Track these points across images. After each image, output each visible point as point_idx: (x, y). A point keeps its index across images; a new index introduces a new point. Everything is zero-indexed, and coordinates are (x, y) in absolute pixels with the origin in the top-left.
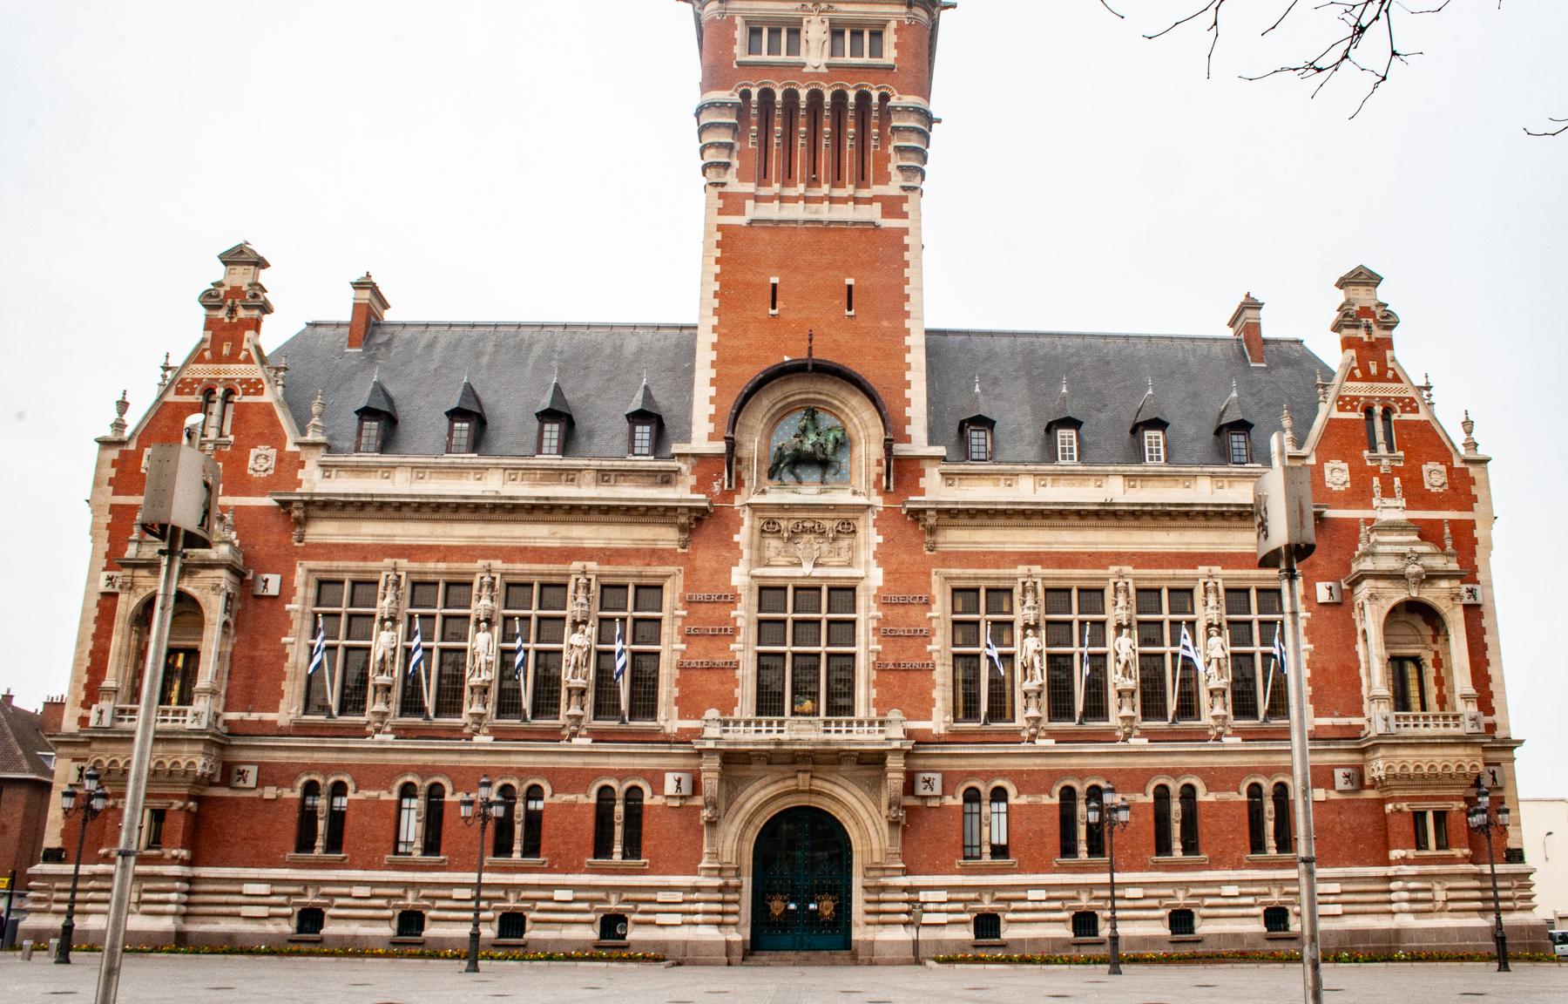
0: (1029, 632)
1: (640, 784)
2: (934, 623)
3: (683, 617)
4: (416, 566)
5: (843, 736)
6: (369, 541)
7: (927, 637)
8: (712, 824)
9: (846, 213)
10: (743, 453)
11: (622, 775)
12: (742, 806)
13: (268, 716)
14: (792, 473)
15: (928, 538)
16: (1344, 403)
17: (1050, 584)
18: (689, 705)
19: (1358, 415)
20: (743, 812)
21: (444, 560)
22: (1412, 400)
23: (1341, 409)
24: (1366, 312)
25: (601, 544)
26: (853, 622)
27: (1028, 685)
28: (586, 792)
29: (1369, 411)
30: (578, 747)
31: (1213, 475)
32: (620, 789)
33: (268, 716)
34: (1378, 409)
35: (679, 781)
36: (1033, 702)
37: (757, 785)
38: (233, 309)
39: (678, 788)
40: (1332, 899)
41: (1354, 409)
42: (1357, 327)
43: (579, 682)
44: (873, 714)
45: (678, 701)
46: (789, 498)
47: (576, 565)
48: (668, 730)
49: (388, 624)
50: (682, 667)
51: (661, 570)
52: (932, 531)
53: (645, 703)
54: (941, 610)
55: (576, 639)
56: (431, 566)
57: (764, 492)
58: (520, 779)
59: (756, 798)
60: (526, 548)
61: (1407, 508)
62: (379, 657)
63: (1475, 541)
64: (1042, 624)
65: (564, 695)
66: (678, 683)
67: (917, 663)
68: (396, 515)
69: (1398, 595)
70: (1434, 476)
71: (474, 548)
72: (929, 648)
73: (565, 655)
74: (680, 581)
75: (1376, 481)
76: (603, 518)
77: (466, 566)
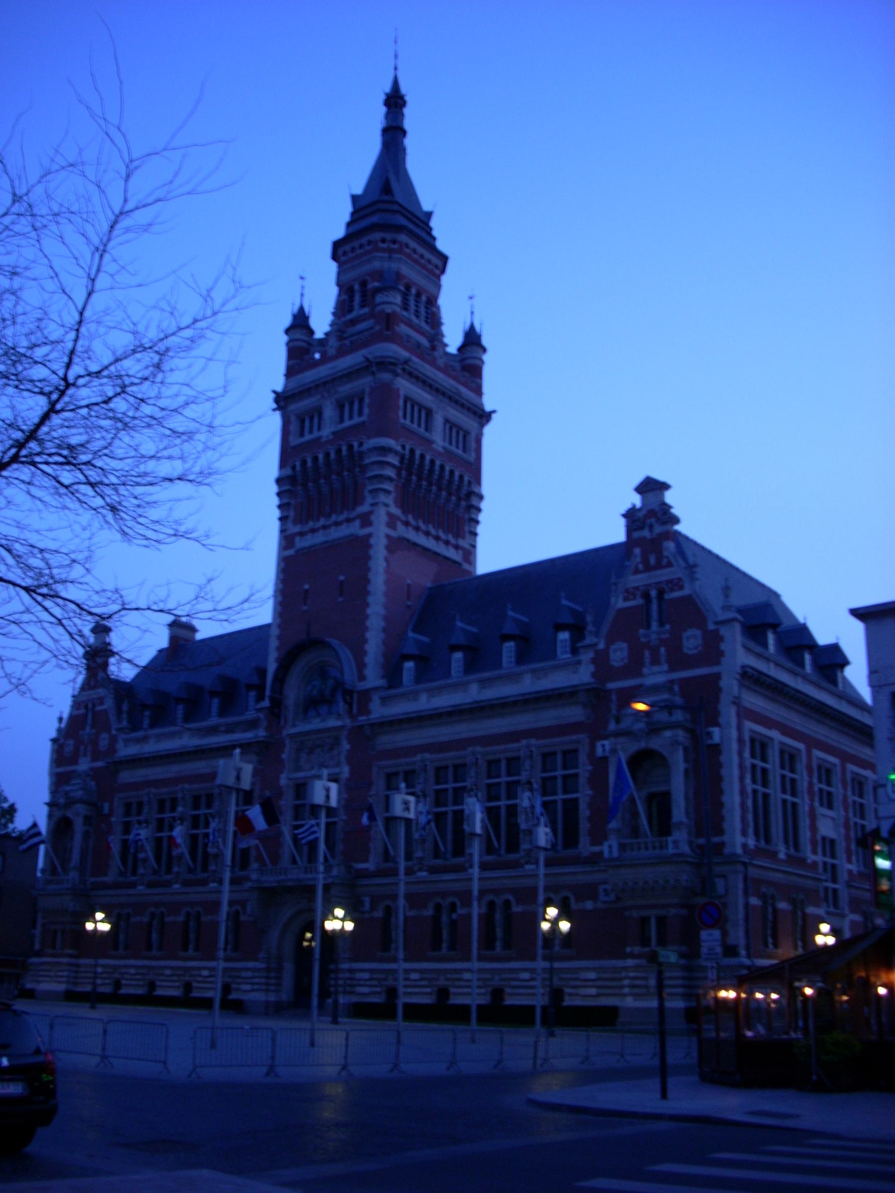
9: (344, 531)
13: (105, 879)
16: (629, 594)
19: (639, 601)
22: (680, 579)
23: (626, 599)
24: (651, 513)
29: (646, 596)
31: (533, 671)
33: (105, 879)
34: (653, 593)
38: (98, 656)
41: (634, 599)
42: (642, 528)
46: (307, 727)
61: (672, 669)
63: (720, 690)
69: (634, 747)
70: (692, 641)
75: (647, 654)
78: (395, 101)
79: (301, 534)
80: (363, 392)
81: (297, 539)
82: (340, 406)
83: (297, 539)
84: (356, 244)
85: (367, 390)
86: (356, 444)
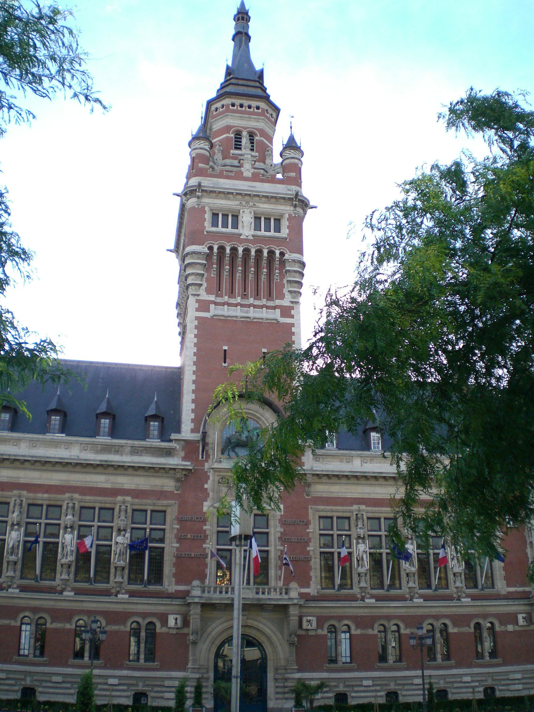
0: (360, 541)
1: (154, 620)
2: (311, 535)
3: (177, 528)
4: (31, 495)
5: (266, 596)
6: (5, 480)
7: (307, 543)
8: (195, 643)
9: (264, 314)
10: (209, 440)
11: (144, 615)
12: (210, 634)
14: (234, 452)
15: (307, 489)
17: (370, 515)
18: (180, 578)
20: (210, 637)
21: (47, 492)
25: (133, 487)
26: (267, 533)
27: (360, 570)
28: (124, 623)
30: (121, 598)
32: (144, 623)
35: (176, 619)
36: (363, 579)
37: (218, 622)
39: (176, 623)
40: (517, 682)
43: (122, 563)
44: (281, 584)
45: (175, 575)
47: (120, 498)
48: (170, 591)
49: (16, 527)
50: (178, 557)
51: (165, 502)
52: (309, 485)
53: (157, 575)
54: (314, 528)
55: (120, 539)
56: (40, 495)
57: (220, 462)
58: (89, 617)
59: (217, 630)
60: (92, 488)
62: (11, 545)
64: (366, 536)
65: (112, 570)
66: (175, 565)
67: (302, 557)
68: (21, 466)
71: (63, 487)
72: (308, 548)
73: (113, 548)
74: (176, 509)
76: (135, 473)
77: (59, 496)
78: (242, 16)
79: (216, 304)
80: (282, 216)
81: (212, 306)
82: (257, 219)
83: (212, 306)
84: (246, 103)
85: (287, 216)
86: (277, 253)
